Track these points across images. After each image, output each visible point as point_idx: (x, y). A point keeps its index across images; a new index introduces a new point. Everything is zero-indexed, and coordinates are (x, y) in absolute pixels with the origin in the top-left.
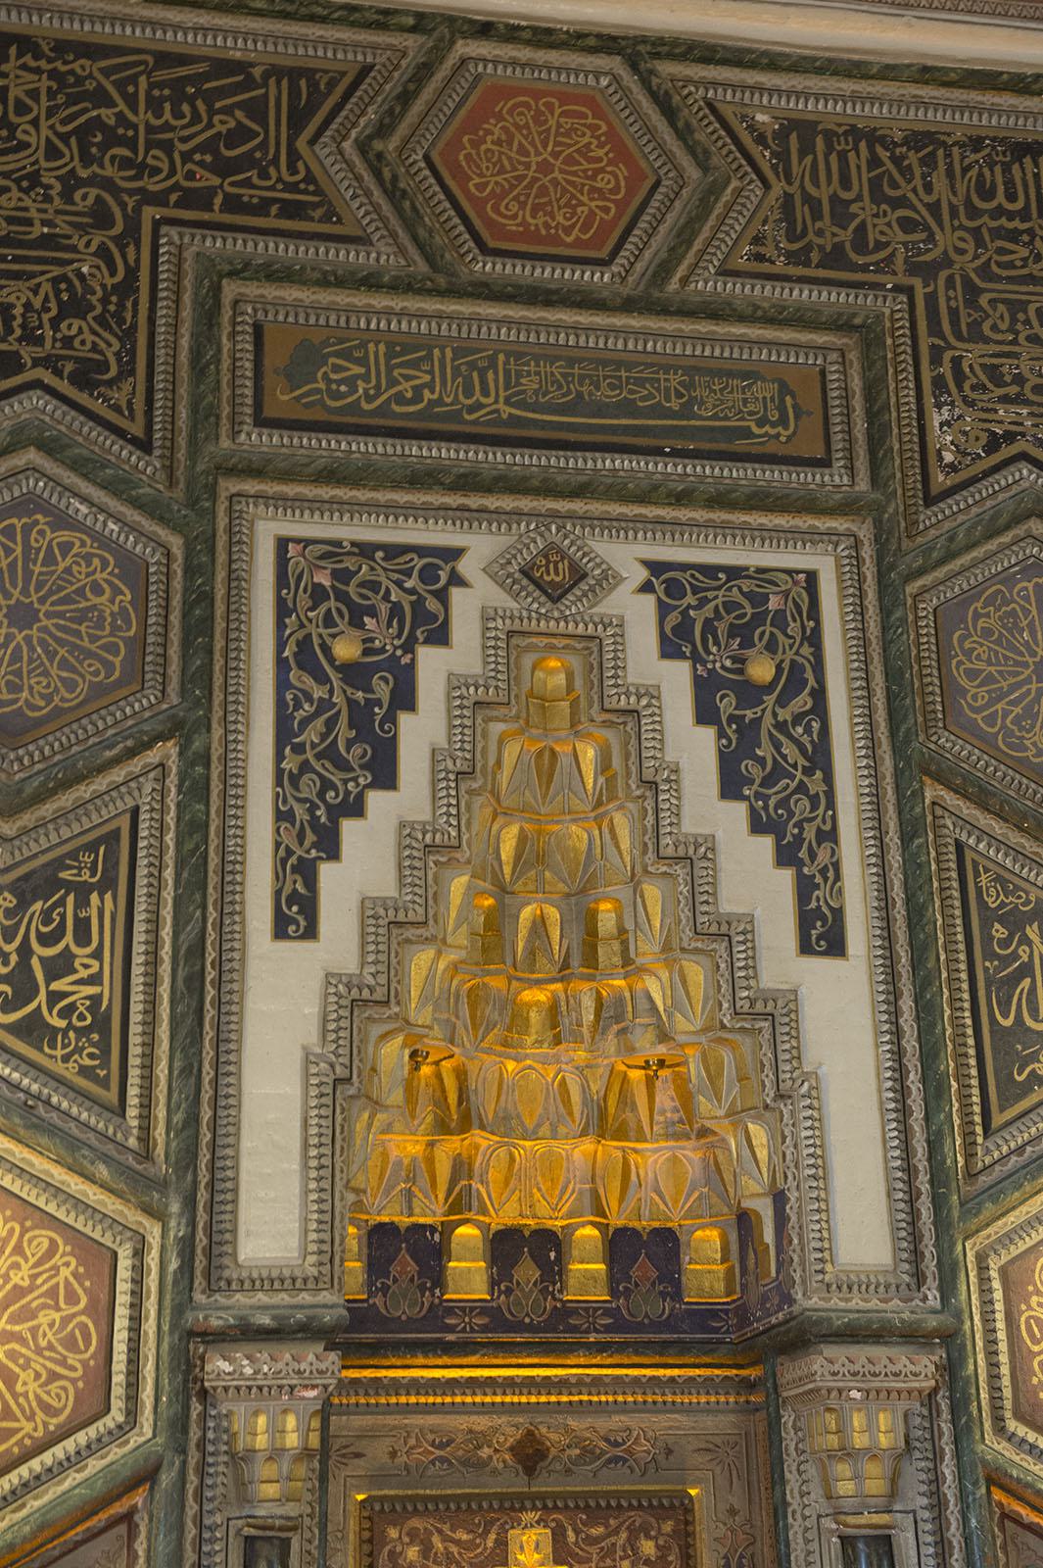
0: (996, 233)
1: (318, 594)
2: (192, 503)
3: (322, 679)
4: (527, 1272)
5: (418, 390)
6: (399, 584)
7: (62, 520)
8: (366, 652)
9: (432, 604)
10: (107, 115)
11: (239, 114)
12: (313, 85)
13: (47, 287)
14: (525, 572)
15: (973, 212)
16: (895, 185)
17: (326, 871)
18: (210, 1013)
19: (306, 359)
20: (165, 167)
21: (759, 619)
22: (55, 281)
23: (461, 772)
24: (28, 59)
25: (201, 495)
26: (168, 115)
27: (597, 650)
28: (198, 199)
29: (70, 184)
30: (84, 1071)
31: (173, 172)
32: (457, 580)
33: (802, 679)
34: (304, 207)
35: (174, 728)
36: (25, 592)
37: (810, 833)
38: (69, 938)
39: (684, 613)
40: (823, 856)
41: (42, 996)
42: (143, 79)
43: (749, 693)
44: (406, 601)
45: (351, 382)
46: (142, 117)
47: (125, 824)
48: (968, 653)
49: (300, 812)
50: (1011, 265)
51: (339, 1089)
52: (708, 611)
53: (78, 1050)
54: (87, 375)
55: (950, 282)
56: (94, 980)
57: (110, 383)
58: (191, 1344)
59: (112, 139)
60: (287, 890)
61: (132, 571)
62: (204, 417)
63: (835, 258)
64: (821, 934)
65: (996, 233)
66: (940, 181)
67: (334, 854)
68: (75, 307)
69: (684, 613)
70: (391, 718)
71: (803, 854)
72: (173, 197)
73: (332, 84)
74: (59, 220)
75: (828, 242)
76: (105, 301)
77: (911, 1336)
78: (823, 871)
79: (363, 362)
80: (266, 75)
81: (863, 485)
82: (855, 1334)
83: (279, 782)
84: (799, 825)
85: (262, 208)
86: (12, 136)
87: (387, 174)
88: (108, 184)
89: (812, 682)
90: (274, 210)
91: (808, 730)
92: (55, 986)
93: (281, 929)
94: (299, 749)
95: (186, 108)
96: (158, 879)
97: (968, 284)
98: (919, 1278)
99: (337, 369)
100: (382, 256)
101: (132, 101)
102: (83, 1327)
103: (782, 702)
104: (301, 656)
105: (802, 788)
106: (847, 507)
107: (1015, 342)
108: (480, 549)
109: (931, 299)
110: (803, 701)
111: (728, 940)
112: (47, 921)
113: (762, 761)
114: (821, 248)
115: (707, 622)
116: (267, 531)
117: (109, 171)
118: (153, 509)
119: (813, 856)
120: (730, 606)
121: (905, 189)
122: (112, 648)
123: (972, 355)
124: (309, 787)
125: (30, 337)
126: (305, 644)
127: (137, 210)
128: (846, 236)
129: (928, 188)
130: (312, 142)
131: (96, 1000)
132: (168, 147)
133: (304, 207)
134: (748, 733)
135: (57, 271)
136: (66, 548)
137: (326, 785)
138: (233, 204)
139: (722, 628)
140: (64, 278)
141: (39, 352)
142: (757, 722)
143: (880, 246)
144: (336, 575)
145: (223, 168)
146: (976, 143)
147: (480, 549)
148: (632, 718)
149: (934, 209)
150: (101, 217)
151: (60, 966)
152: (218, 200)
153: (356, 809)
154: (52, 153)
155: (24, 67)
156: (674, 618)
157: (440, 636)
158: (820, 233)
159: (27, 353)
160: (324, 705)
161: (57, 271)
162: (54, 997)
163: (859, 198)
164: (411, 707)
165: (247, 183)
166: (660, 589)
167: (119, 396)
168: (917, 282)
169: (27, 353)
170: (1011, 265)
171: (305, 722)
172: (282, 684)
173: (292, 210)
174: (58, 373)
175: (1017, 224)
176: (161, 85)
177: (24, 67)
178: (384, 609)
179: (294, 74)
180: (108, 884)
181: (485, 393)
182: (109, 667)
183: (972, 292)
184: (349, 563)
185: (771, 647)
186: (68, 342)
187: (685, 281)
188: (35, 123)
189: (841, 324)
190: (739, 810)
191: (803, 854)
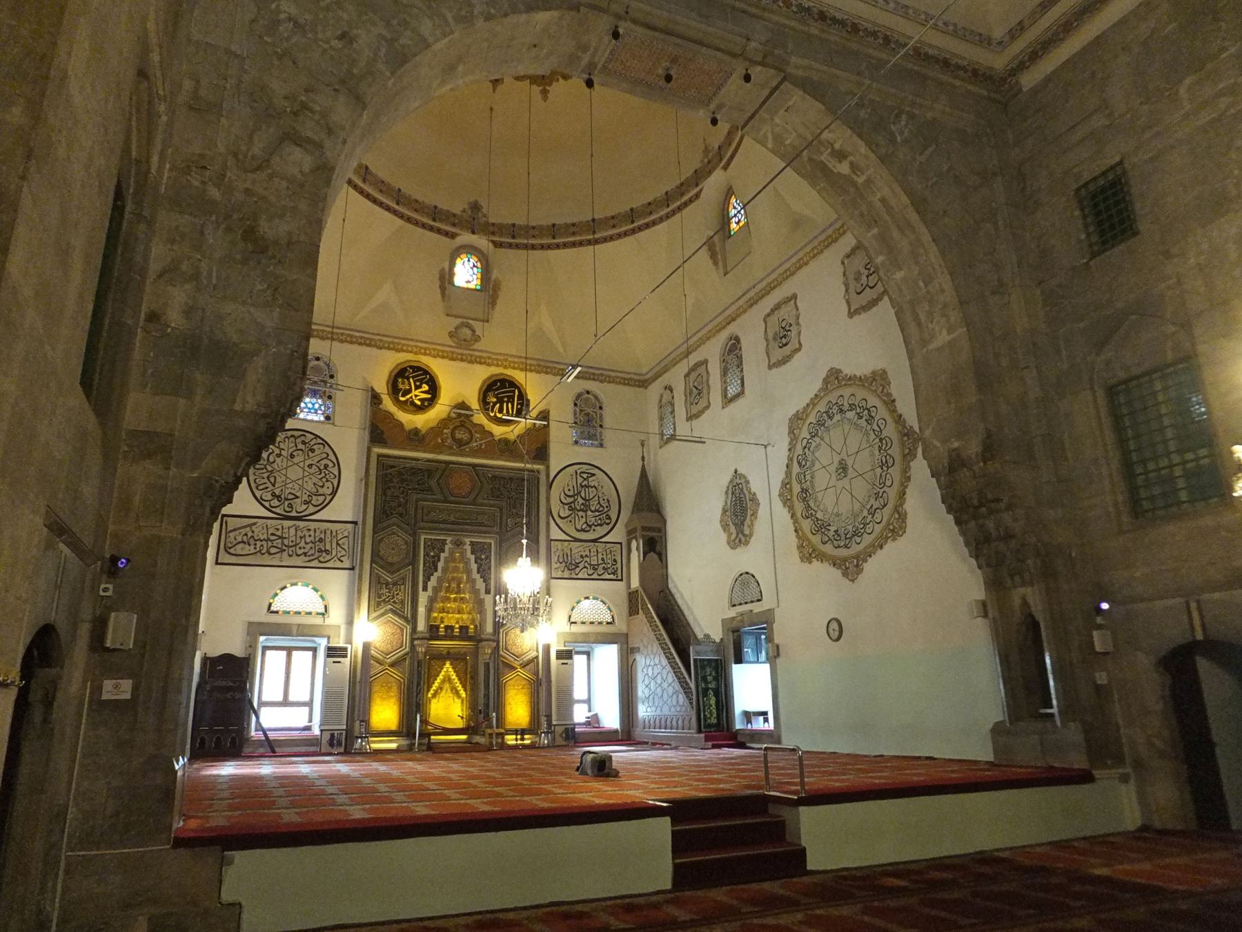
19: (428, 513)
23: (445, 570)
27: (463, 554)
34: (430, 490)
51: (430, 610)
54: (401, 515)
61: (406, 543)
96: (409, 584)
100: (439, 496)
104: (427, 554)
108: (449, 539)
111: (475, 592)
116: (423, 537)
133: (430, 490)
147: (449, 539)
148: (467, 563)
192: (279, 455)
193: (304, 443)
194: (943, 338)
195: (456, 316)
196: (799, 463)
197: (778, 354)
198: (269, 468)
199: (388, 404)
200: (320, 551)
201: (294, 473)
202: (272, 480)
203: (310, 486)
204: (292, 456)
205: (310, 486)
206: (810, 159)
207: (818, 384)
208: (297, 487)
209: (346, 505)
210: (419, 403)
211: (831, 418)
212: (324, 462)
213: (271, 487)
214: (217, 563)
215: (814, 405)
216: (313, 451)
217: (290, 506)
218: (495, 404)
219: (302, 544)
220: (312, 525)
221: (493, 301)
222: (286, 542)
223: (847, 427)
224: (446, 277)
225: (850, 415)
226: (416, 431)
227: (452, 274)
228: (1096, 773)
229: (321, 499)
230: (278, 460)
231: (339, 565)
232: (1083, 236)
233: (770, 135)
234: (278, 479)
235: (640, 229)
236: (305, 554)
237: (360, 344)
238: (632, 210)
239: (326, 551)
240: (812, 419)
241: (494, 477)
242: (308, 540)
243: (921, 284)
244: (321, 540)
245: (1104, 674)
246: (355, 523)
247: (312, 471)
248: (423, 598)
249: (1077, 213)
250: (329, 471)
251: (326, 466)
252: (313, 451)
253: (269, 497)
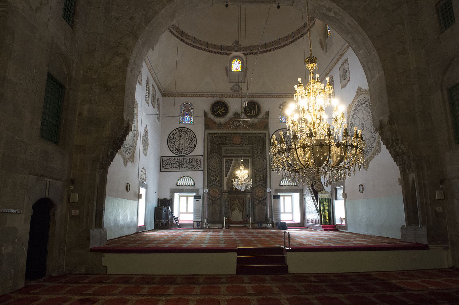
1: (227, 162)
7: (216, 159)
28: (221, 143)
35: (221, 168)
58: (222, 193)
61: (219, 161)
63: (250, 143)
67: (227, 173)
82: (249, 192)
108: (234, 159)
116: (225, 159)
123: (257, 148)
138: (223, 143)
146: (258, 137)
151: (217, 178)
157: (232, 163)
180: (218, 175)
192: (177, 136)
193: (184, 131)
194: (377, 76)
195: (232, 82)
196: (350, 125)
197: (344, 82)
198: (174, 141)
199: (211, 116)
200: (191, 165)
201: (182, 141)
202: (175, 144)
203: (187, 145)
204: (181, 136)
205: (187, 145)
206: (319, 13)
207: (355, 94)
208: (183, 146)
209: (199, 150)
210: (222, 114)
211: (359, 107)
212: (191, 137)
213: (175, 147)
214: (160, 171)
215: (354, 102)
216: (187, 134)
217: (181, 152)
218: (249, 111)
219: (186, 164)
220: (189, 158)
221: (246, 75)
222: (181, 163)
223: (363, 110)
224: (228, 69)
225: (364, 105)
226: (220, 124)
227: (230, 66)
228: (430, 246)
229: (191, 149)
230: (177, 138)
231: (198, 169)
232: (438, 25)
233: (302, 7)
234: (177, 143)
235: (296, 40)
236: (187, 167)
237: (201, 97)
238: (293, 33)
239: (193, 165)
240: (354, 108)
241: (249, 137)
242: (187, 162)
243: (368, 55)
244: (191, 162)
245: (441, 208)
246: (202, 156)
247: (187, 140)
249: (436, 15)
250: (193, 140)
251: (192, 138)
252: (187, 134)
253: (175, 150)
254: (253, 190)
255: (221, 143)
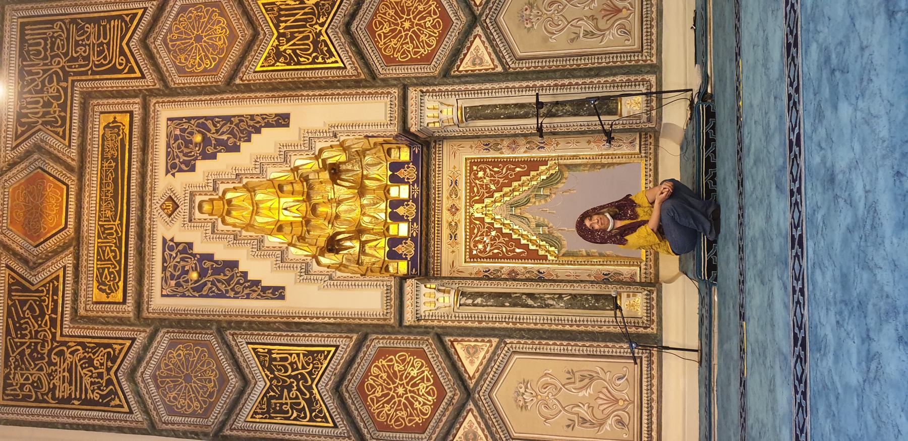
0: (52, 50)
1: (178, 285)
2: (149, 325)
3: (205, 284)
4: (401, 211)
5: (112, 251)
6: (174, 258)
8: (196, 270)
9: (180, 247)
10: (28, 352)
11: (24, 309)
12: (13, 284)
13: (85, 371)
14: (170, 216)
15: (45, 58)
16: (37, 85)
17: (264, 284)
18: (308, 320)
20: (43, 333)
21: (183, 138)
22: (83, 369)
24: (11, 377)
25: (147, 322)
26: (26, 332)
28: (53, 322)
29: (50, 363)
30: (325, 358)
31: (45, 331)
32: (172, 240)
33: (202, 123)
36: (181, 377)
37: (251, 123)
38: (286, 363)
39: (181, 163)
40: (259, 119)
41: (303, 371)
42: (16, 340)
43: (206, 141)
44: (179, 256)
45: (110, 273)
46: (27, 340)
47: (251, 346)
48: (193, 66)
49: (246, 291)
50: (63, 45)
52: (180, 155)
53: (319, 360)
55: (70, 67)
56: (298, 355)
57: (114, 351)
58: (400, 327)
59: (35, 350)
60: (270, 295)
62: (121, 321)
63: (63, 107)
64: (282, 120)
65: (52, 50)
66: (34, 70)
68: (90, 362)
69: (181, 163)
70: (217, 262)
71: (258, 125)
72: (53, 330)
73: (13, 278)
74: (62, 367)
75: (57, 109)
76: (88, 353)
77: (404, 99)
78: (263, 119)
79: (104, 269)
80: (12, 300)
81: (137, 100)
83: (238, 298)
84: (249, 126)
85: (55, 302)
86: (36, 382)
87: (40, 261)
88: (50, 351)
89: (202, 120)
90: (55, 297)
91: (218, 122)
92: (300, 367)
93: (282, 297)
94: (227, 291)
95: (24, 326)
97: (68, 61)
98: (389, 93)
99: (106, 278)
101: (23, 344)
102: (399, 357)
103: (209, 131)
105: (237, 125)
106: (145, 107)
107: (89, 45)
109: (76, 74)
110: (209, 124)
112: (280, 370)
113: (229, 138)
114: (60, 112)
115: (184, 155)
117: (46, 351)
118: (152, 338)
119: (259, 122)
120: (179, 148)
121: (38, 81)
122: (197, 350)
124: (239, 288)
125: (100, 375)
126: (194, 289)
127: (58, 342)
128: (55, 104)
129: (38, 73)
130: (33, 285)
131: (304, 355)
132: (37, 332)
134: (220, 143)
135: (79, 368)
136: (167, 365)
137: (238, 283)
139: (186, 150)
140: (81, 366)
141: (105, 374)
142: (216, 139)
143: (58, 91)
144: (172, 279)
145: (42, 314)
149: (45, 71)
150: (61, 354)
152: (53, 316)
153: (245, 274)
154: (41, 369)
155: (14, 378)
156: (183, 167)
157: (190, 245)
158: (55, 112)
159: (106, 377)
160: (213, 283)
161: (79, 368)
162: (304, 368)
163: (42, 98)
164: (212, 255)
165: (47, 306)
166: (174, 171)
167: (118, 347)
168: (70, 79)
169: (106, 377)
170: (63, 45)
171: (219, 289)
172: (207, 296)
173: (55, 292)
174: (112, 367)
175: (49, 42)
176: (17, 335)
177: (14, 378)
178: (182, 263)
179: (10, 291)
181: (112, 228)
182: (203, 351)
183: (74, 59)
184: (168, 274)
185: (192, 134)
186: (102, 364)
187: (73, 160)
188: (32, 375)
189: (84, 107)
190: (244, 146)
191: (258, 125)
248: (308, 298)
254: (387, 82)
255: (53, 322)
